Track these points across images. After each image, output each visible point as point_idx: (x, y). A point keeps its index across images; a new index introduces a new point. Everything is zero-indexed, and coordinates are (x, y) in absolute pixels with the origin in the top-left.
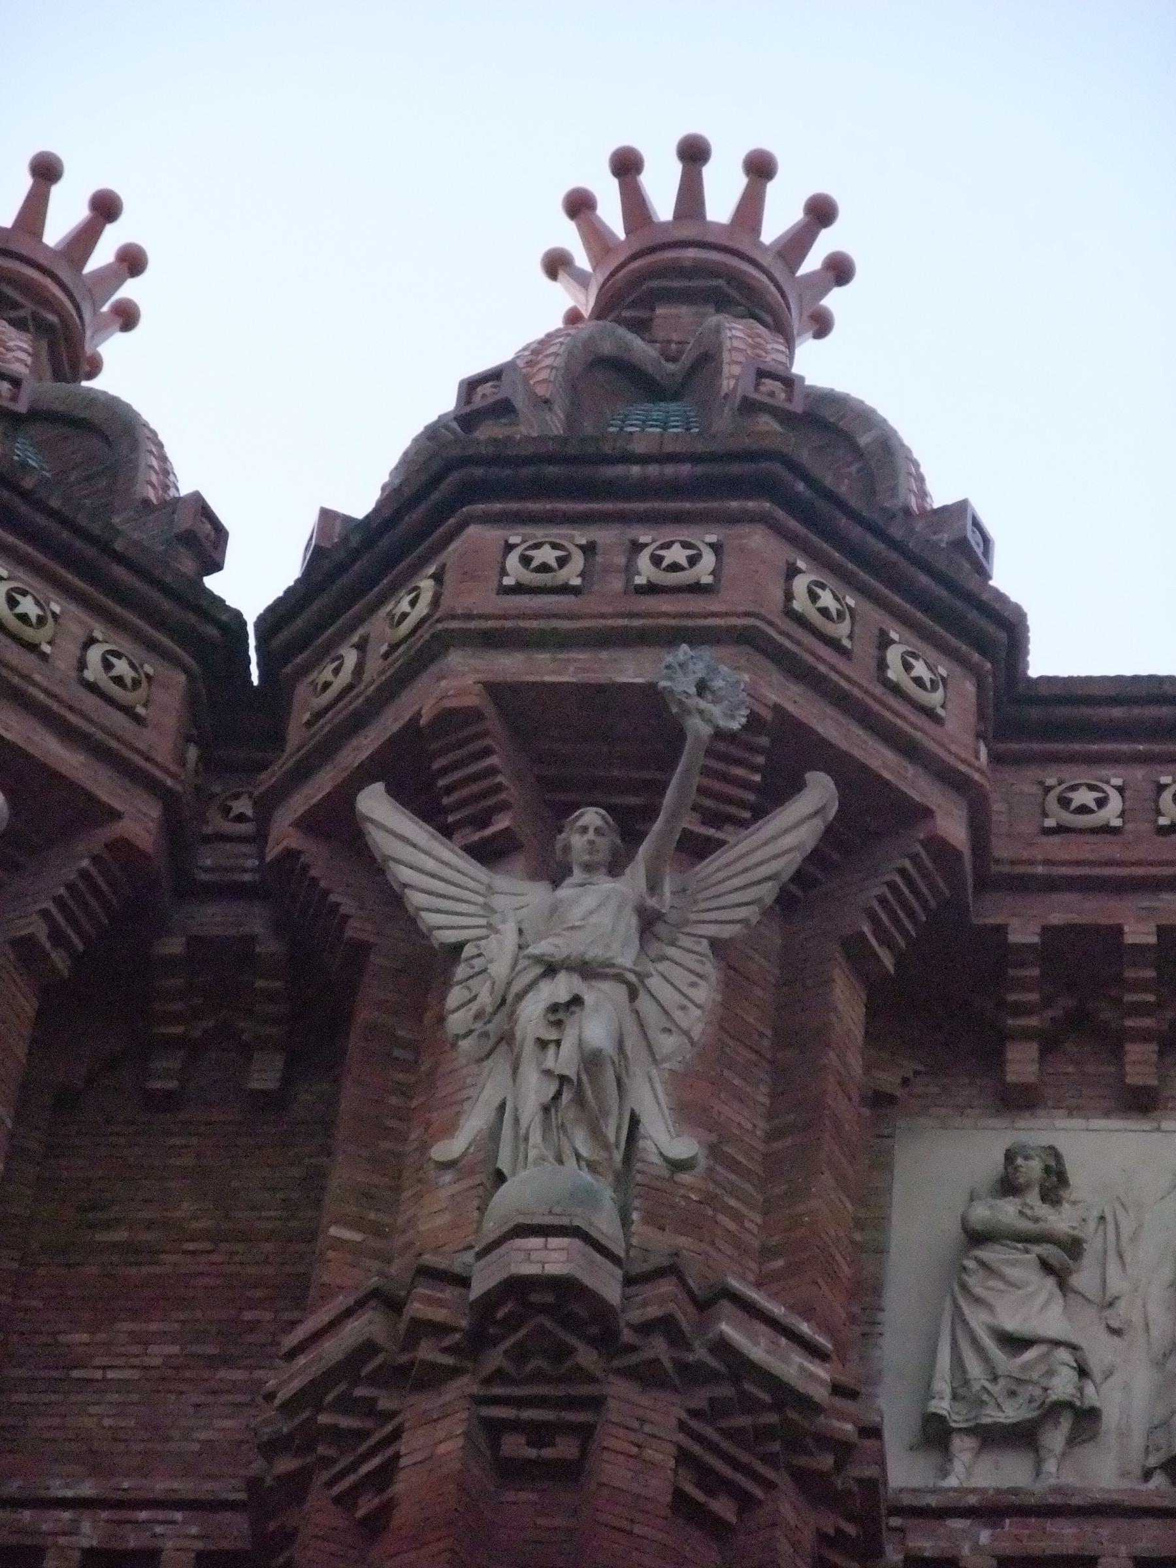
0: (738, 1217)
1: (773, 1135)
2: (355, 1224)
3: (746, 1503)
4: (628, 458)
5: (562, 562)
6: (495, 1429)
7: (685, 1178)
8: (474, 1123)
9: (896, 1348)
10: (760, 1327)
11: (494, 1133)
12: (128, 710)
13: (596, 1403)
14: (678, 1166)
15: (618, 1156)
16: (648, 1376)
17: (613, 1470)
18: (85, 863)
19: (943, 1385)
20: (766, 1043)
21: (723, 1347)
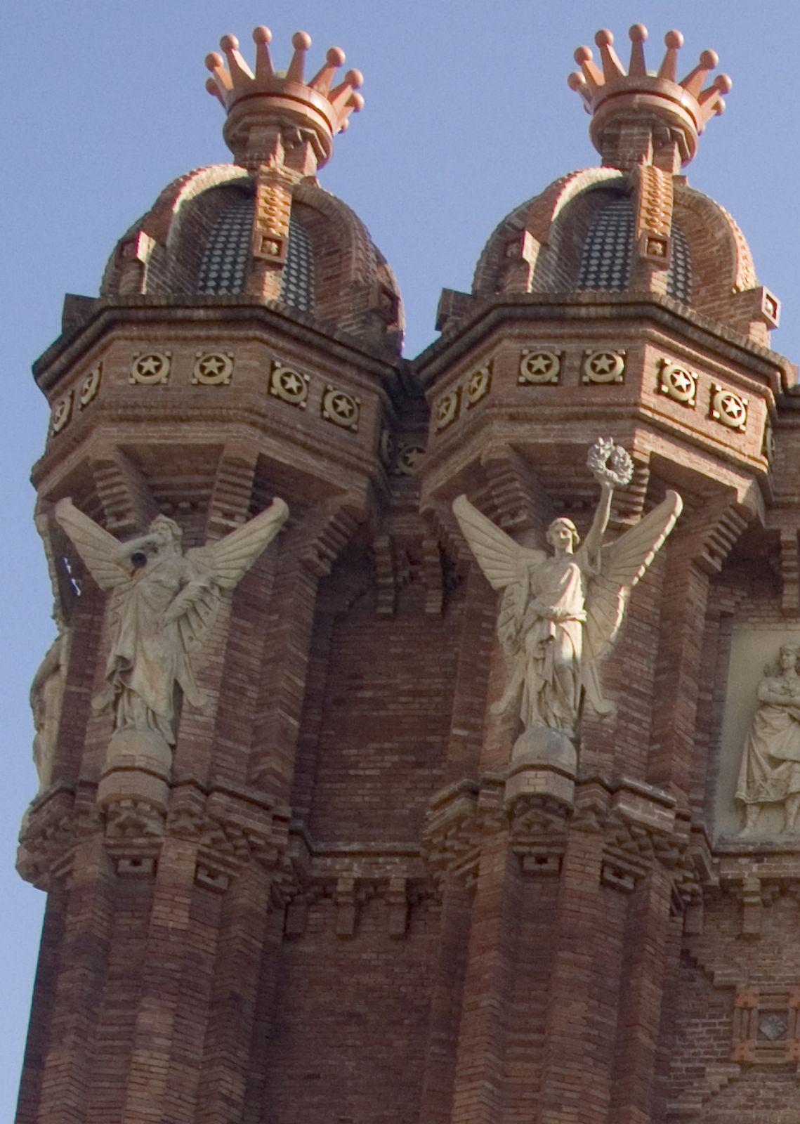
0: (639, 722)
1: (658, 672)
2: (463, 726)
3: (637, 879)
4: (580, 305)
5: (548, 367)
6: (521, 857)
7: (607, 720)
8: (510, 692)
9: (724, 757)
10: (639, 799)
11: (519, 699)
12: (347, 428)
13: (564, 844)
14: (604, 716)
15: (575, 713)
16: (588, 831)
17: (572, 881)
18: (332, 518)
19: (742, 783)
20: (657, 618)
21: (620, 815)
